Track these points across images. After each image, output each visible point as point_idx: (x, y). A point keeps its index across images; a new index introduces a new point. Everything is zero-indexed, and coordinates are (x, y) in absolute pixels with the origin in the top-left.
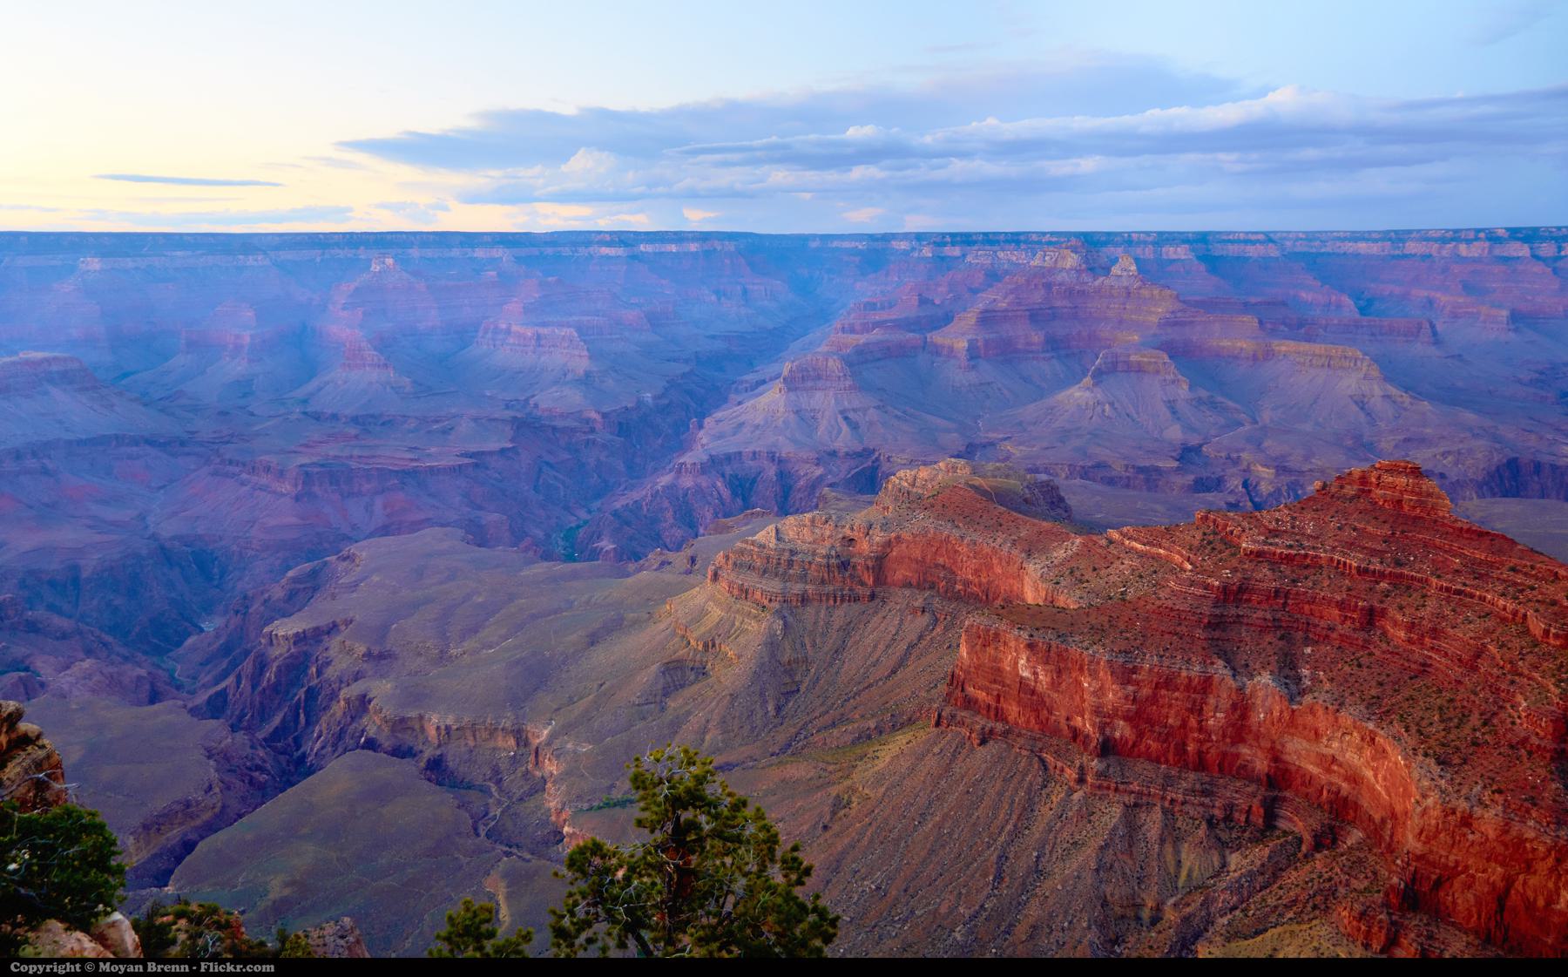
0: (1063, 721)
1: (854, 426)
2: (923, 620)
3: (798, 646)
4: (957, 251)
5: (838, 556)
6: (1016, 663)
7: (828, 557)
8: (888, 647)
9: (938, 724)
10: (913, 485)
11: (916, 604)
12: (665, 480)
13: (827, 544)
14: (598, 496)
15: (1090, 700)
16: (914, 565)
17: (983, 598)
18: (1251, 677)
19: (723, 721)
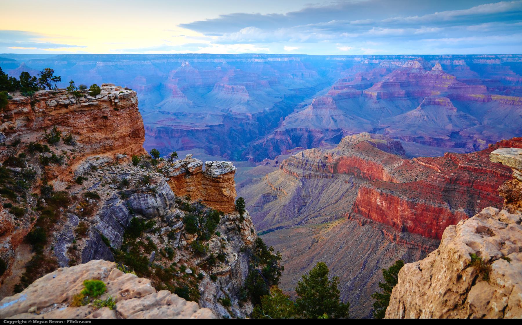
0: (390, 220)
1: (335, 121)
2: (349, 185)
3: (307, 191)
4: (377, 62)
5: (322, 163)
6: (376, 200)
7: (319, 163)
8: (336, 193)
9: (349, 218)
10: (351, 141)
11: (347, 180)
12: (271, 136)
13: (319, 159)
14: (249, 141)
15: (400, 213)
16: (347, 167)
17: (370, 179)
18: (457, 209)
19: (281, 213)
